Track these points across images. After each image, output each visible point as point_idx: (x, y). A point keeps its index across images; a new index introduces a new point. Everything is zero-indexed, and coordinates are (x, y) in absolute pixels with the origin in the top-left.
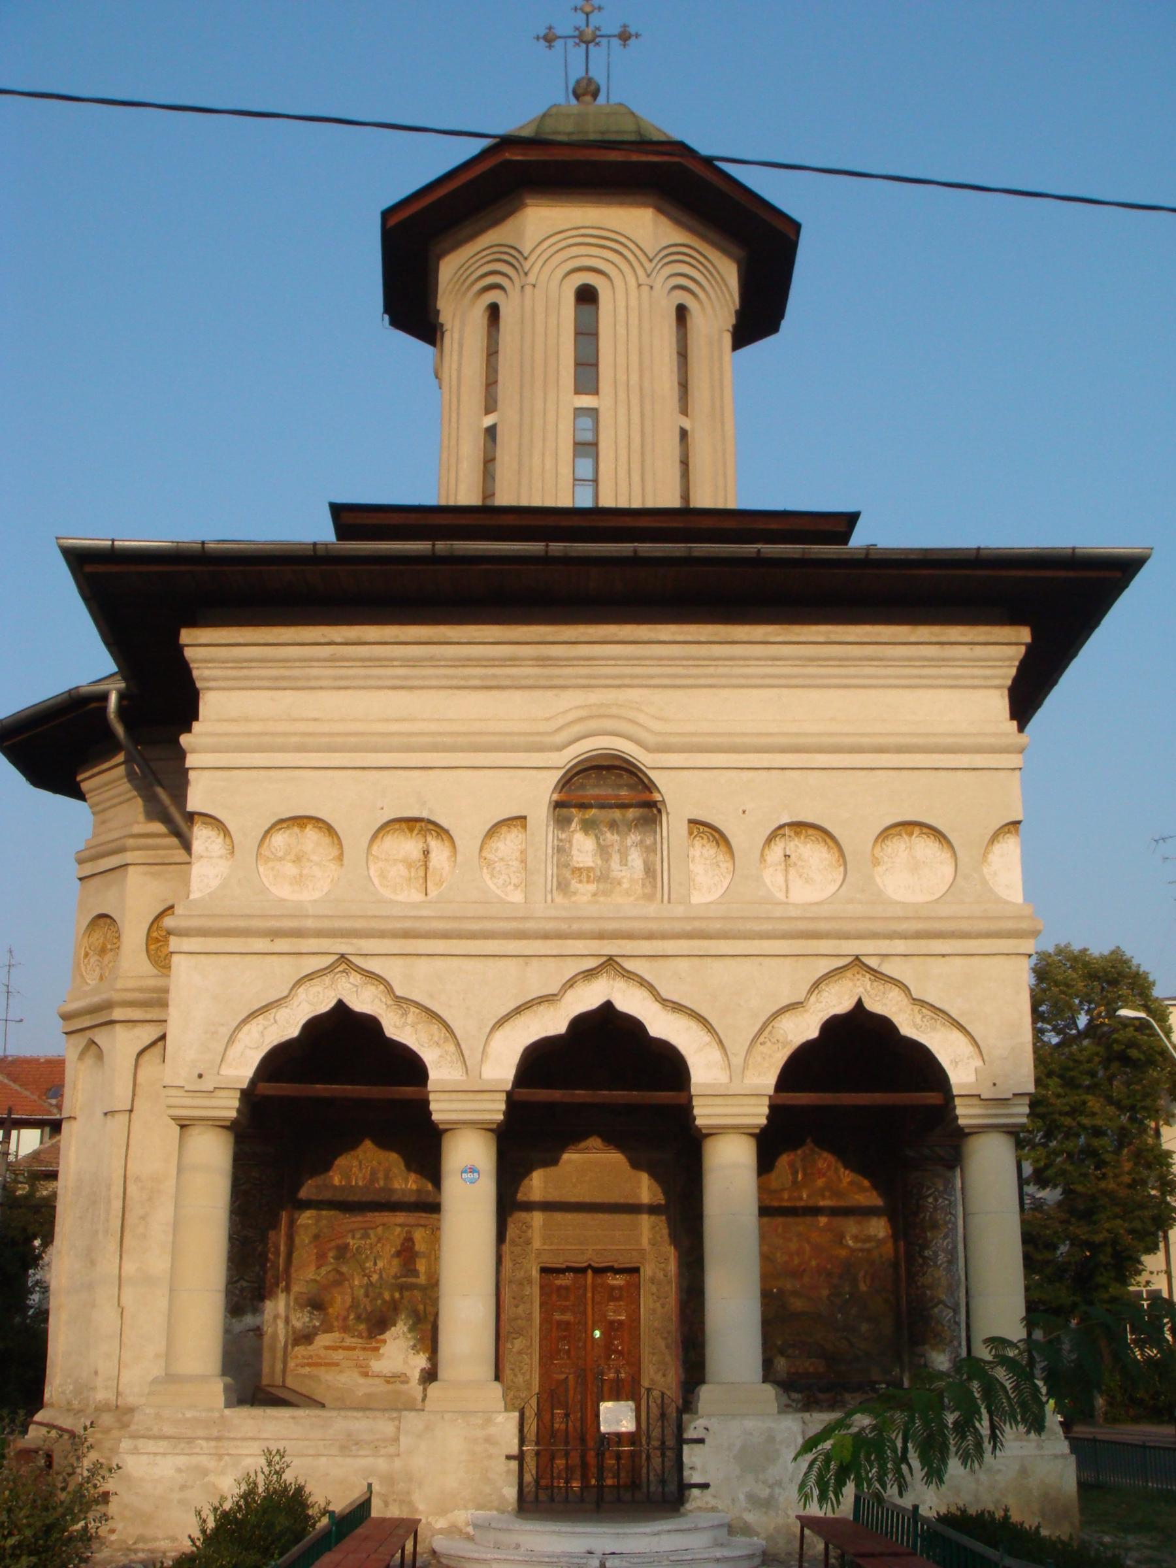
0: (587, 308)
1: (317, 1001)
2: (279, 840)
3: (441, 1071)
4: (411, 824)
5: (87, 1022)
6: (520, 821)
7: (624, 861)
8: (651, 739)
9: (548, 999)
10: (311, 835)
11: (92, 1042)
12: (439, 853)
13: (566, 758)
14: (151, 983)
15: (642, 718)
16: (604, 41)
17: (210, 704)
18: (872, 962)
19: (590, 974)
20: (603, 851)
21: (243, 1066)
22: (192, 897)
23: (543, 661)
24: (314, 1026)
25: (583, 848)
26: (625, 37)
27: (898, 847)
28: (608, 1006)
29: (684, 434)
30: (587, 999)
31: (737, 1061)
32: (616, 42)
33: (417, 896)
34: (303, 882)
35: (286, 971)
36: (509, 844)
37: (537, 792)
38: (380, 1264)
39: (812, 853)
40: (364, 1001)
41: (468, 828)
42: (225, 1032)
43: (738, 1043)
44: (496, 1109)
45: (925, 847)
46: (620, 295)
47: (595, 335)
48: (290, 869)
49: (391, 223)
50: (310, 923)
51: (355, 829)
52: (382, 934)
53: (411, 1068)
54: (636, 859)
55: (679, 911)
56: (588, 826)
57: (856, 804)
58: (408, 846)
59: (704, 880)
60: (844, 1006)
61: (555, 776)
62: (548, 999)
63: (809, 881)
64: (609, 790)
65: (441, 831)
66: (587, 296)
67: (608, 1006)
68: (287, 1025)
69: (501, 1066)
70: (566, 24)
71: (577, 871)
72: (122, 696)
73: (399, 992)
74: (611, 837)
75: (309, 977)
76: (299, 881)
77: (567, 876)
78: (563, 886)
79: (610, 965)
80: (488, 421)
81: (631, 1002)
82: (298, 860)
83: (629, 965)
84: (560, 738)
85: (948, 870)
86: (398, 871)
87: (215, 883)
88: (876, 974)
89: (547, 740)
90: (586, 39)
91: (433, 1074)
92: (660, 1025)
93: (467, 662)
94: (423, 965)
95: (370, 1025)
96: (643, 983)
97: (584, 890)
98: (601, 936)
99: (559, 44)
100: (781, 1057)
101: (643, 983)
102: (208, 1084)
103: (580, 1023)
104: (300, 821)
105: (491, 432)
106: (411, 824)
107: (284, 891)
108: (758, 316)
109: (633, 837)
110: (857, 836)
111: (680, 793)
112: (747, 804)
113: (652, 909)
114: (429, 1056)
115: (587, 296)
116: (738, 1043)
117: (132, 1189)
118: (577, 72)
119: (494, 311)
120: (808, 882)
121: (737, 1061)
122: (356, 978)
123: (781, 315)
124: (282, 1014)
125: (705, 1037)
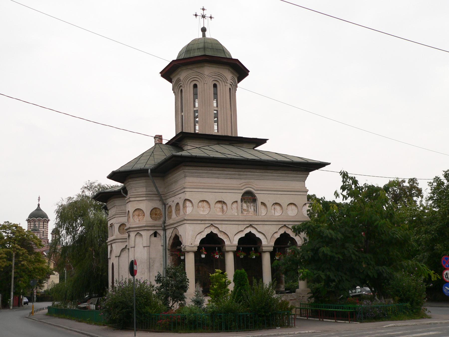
0: (215, 89)
1: (208, 231)
2: (200, 204)
3: (227, 243)
4: (220, 202)
5: (138, 229)
6: (237, 202)
7: (251, 208)
8: (256, 189)
9: (242, 231)
10: (205, 203)
12: (225, 207)
13: (243, 191)
14: (152, 222)
15: (254, 185)
16: (207, 18)
18: (287, 225)
19: (247, 227)
20: (248, 207)
21: (198, 243)
22: (187, 213)
23: (239, 175)
24: (208, 235)
25: (245, 206)
27: (290, 207)
28: (250, 232)
30: (247, 231)
31: (269, 241)
33: (221, 214)
34: (204, 212)
35: (203, 226)
36: (235, 205)
37: (238, 197)
39: (278, 207)
40: (215, 231)
41: (229, 203)
42: (195, 237)
43: (269, 238)
44: (235, 249)
45: (293, 207)
46: (221, 87)
47: (217, 94)
48: (202, 209)
50: (207, 219)
51: (212, 202)
52: (218, 221)
53: (222, 242)
54: (252, 208)
55: (260, 217)
56: (245, 202)
57: (284, 200)
58: (219, 205)
59: (263, 211)
60: (283, 232)
62: (242, 231)
63: (278, 212)
64: (249, 197)
65: (224, 203)
66: (215, 86)
67: (250, 232)
68: (204, 235)
69: (236, 242)
70: (200, 13)
71: (244, 210)
72: (151, 170)
73: (220, 230)
74: (249, 204)
75: (207, 227)
76: (203, 211)
77: (243, 210)
78: (242, 212)
79: (251, 226)
81: (254, 231)
82: (203, 207)
83: (253, 226)
84: (242, 188)
85: (297, 211)
86: (218, 210)
87: (191, 211)
88: (288, 227)
89: (241, 188)
90: (203, 17)
91: (226, 243)
92: (258, 235)
93: (227, 174)
94: (224, 226)
95: (216, 235)
96: (255, 228)
97: (245, 213)
98: (250, 221)
99: (198, 17)
100: (275, 240)
101: (255, 228)
102: (193, 245)
103: (246, 235)
104: (203, 201)
106: (220, 202)
107: (201, 213)
109: (252, 204)
110: (284, 205)
111: (260, 198)
112: (269, 199)
113: (256, 217)
114: (225, 240)
115: (215, 86)
116: (269, 238)
117: (150, 260)
120: (277, 213)
121: (269, 241)
122: (213, 228)
124: (203, 233)
125: (264, 237)
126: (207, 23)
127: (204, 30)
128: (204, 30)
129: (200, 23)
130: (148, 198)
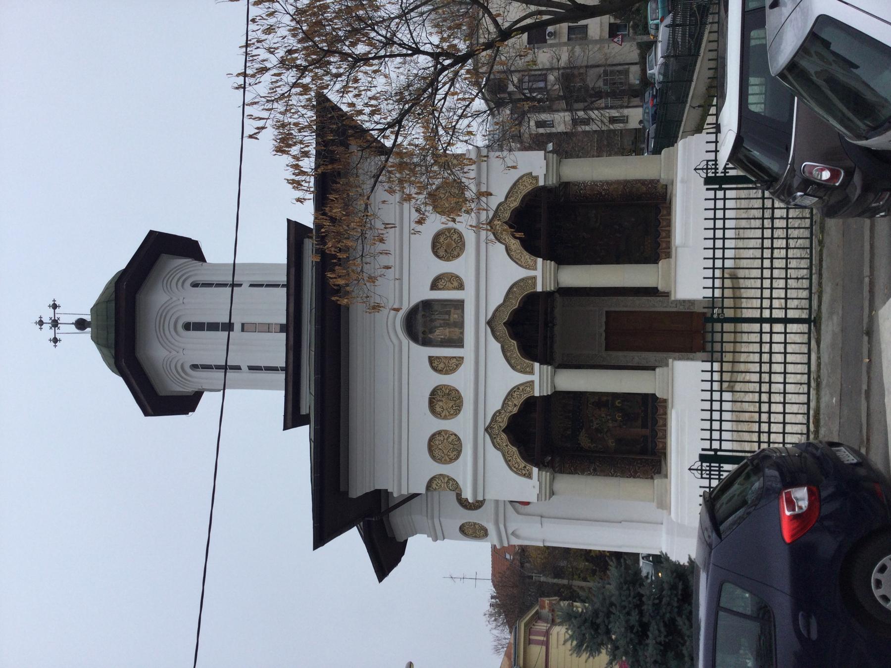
11: (513, 533)
13: (405, 340)
16: (57, 316)
17: (379, 486)
26: (55, 306)
29: (251, 285)
32: (57, 310)
38: (603, 415)
49: (150, 411)
61: (413, 345)
80: (244, 368)
99: (58, 337)
105: (251, 368)
108: (189, 249)
118: (73, 328)
119: (195, 367)
123: (189, 240)
126: (67, 317)
127: (81, 324)
128: (81, 324)
129: (67, 330)
130: (436, 513)
